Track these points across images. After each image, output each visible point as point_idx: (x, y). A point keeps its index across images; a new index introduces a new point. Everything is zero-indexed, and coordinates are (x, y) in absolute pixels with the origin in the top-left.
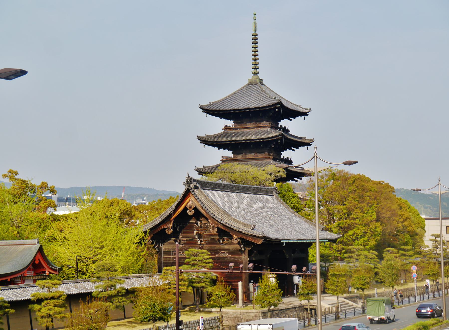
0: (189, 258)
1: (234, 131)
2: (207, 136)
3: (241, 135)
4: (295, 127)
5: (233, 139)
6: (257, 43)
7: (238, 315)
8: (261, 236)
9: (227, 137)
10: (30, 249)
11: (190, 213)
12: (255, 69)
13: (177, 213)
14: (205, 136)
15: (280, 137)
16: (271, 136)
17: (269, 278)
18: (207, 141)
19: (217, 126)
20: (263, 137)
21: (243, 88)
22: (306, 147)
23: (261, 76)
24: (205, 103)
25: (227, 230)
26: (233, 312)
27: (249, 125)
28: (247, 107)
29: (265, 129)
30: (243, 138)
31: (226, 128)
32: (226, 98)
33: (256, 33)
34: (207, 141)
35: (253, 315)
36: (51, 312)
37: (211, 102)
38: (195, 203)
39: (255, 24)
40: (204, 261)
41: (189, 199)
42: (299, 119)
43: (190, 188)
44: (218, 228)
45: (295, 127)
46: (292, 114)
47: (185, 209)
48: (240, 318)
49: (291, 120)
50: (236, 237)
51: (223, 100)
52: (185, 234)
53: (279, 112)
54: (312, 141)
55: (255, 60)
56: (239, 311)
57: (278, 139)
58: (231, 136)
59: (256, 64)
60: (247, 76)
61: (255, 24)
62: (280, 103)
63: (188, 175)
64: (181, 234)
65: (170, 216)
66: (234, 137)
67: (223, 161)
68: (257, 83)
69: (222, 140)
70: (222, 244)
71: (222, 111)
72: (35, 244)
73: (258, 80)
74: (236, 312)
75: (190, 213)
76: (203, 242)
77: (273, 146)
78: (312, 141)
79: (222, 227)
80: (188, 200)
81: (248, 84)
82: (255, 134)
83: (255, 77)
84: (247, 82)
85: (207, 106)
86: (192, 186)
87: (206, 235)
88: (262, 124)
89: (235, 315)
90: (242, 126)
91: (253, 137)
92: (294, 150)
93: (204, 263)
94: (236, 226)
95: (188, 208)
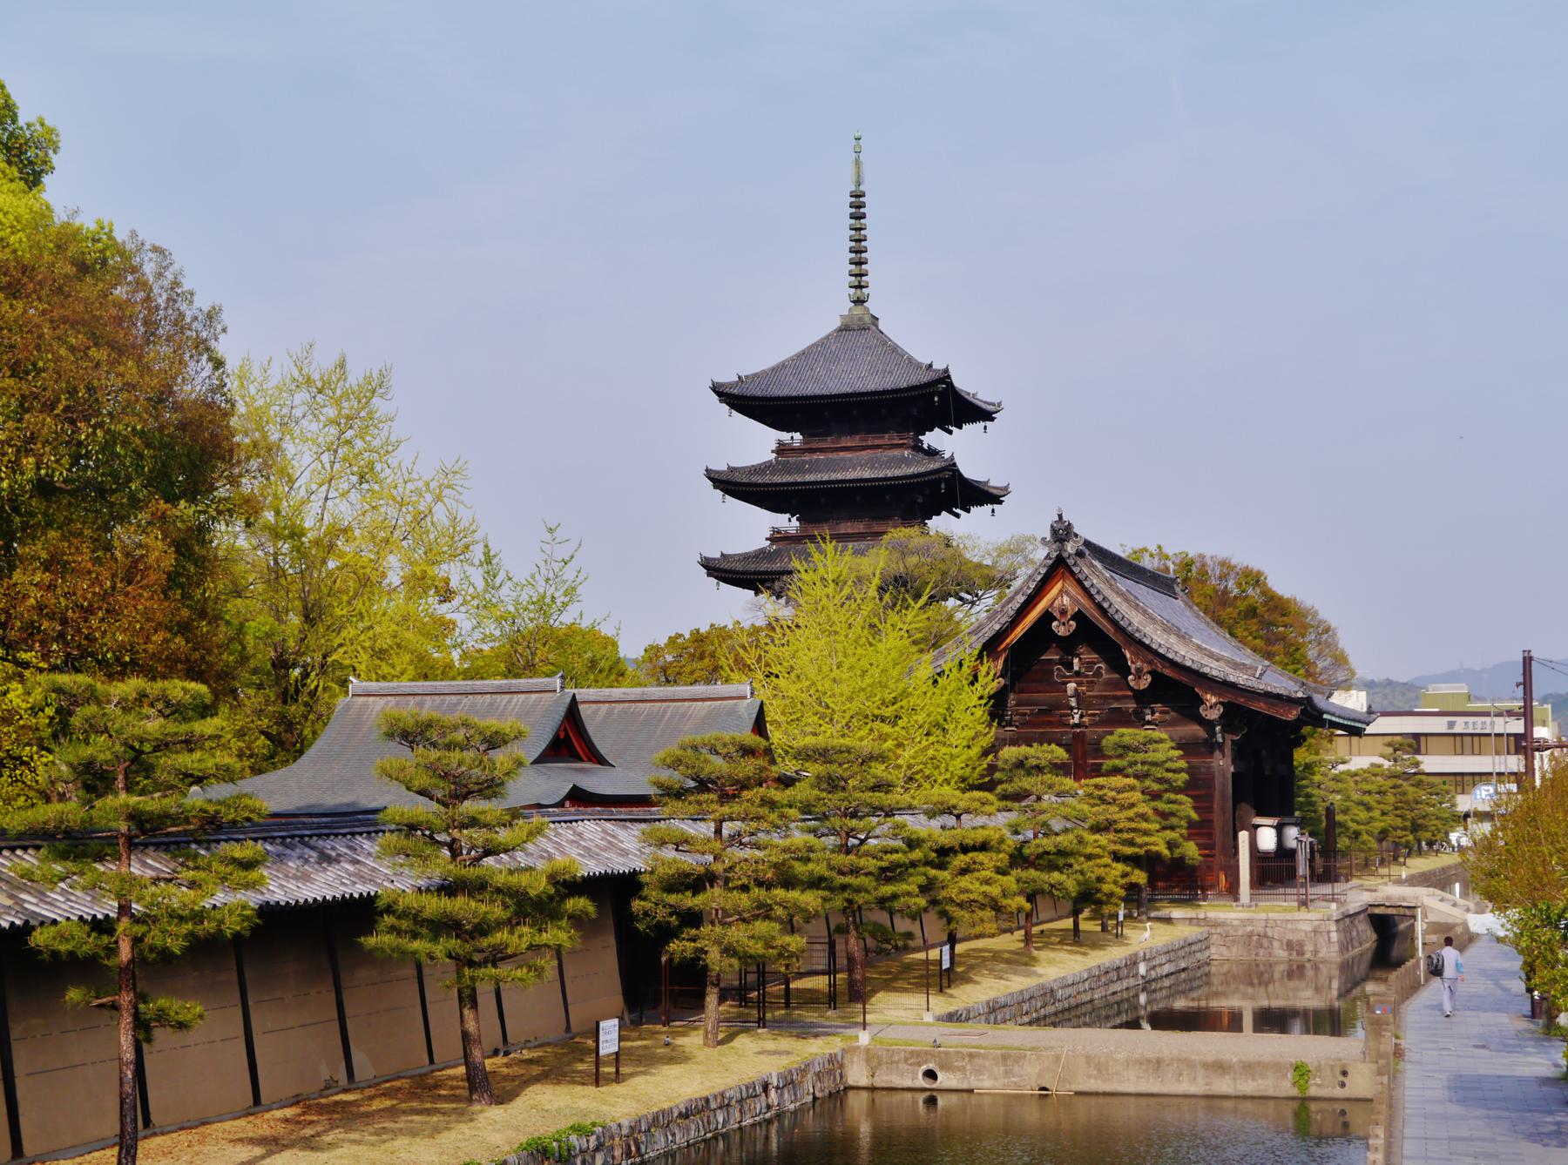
0: (1120, 757)
1: (807, 457)
2: (732, 470)
3: (815, 467)
4: (962, 448)
5: (809, 478)
6: (863, 216)
7: (1260, 930)
8: (1300, 695)
9: (789, 473)
10: (733, 712)
11: (1062, 628)
12: (860, 287)
13: (1020, 631)
14: (725, 468)
15: (947, 475)
16: (923, 470)
17: (1257, 826)
18: (733, 485)
19: (757, 444)
20: (898, 472)
21: (827, 338)
22: (988, 508)
23: (873, 306)
24: (727, 377)
25: (1185, 679)
26: (1242, 921)
27: (846, 441)
28: (850, 390)
29: (897, 452)
30: (840, 476)
31: (782, 449)
32: (783, 365)
33: (862, 188)
34: (733, 485)
35: (1307, 927)
36: (994, 891)
37: (743, 374)
38: (1077, 601)
39: (857, 162)
40: (1169, 765)
41: (1059, 585)
42: (972, 430)
43: (1065, 555)
44: (1153, 673)
45: (962, 448)
46: (960, 410)
47: (1047, 617)
48: (1265, 936)
49: (950, 432)
50: (1214, 700)
51: (774, 369)
52: (1025, 696)
53: (944, 403)
54: (1006, 490)
55: (859, 263)
56: (1263, 916)
57: (939, 481)
58: (799, 469)
59: (861, 275)
60: (832, 310)
61: (857, 162)
62: (945, 378)
63: (1060, 516)
64: (1012, 696)
65: (999, 636)
66: (810, 471)
67: (772, 539)
68: (859, 328)
69: (777, 479)
70: (1149, 723)
71: (779, 398)
72: (744, 698)
73: (867, 319)
74: (1250, 921)
75: (1061, 629)
76: (1085, 719)
77: (920, 500)
78: (1006, 490)
79: (1167, 672)
80: (1054, 591)
81: (840, 330)
82: (871, 464)
83: (858, 310)
84: (837, 324)
85: (731, 385)
86: (1070, 548)
87: (1096, 697)
88: (886, 439)
89: (1249, 929)
90: (828, 443)
91: (867, 474)
92: (958, 516)
93: (1168, 770)
94: (1214, 669)
95: (1057, 614)
